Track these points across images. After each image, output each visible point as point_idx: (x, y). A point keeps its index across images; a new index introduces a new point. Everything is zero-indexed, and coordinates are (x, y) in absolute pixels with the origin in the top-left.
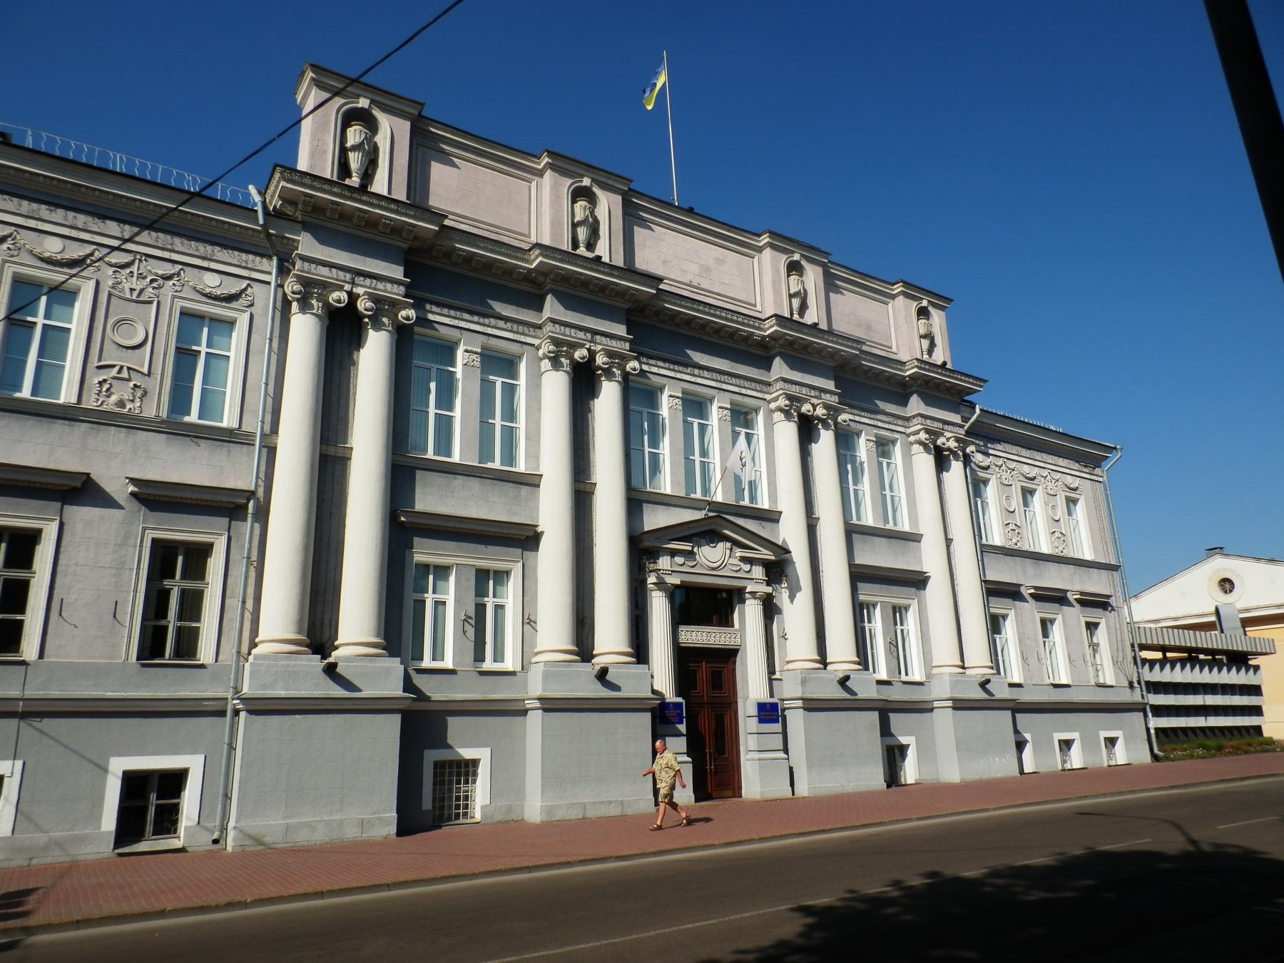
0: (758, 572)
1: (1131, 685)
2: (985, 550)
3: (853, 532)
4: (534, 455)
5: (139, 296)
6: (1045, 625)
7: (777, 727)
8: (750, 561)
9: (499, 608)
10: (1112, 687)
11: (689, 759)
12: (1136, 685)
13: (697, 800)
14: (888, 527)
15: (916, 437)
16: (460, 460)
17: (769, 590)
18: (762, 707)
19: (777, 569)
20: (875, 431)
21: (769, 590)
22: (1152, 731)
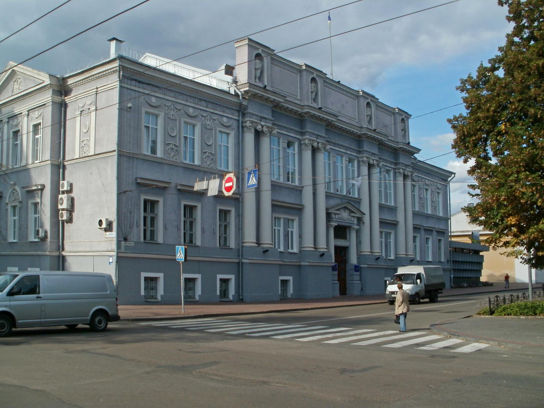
0: (356, 222)
1: (448, 261)
2: (415, 214)
3: (381, 207)
4: (300, 180)
5: (210, 127)
6: (427, 239)
7: (358, 273)
8: (354, 217)
9: (292, 232)
10: (443, 262)
11: (338, 282)
12: (449, 262)
13: (340, 295)
14: (388, 204)
15: (399, 171)
16: (283, 182)
17: (358, 227)
18: (356, 267)
19: (360, 220)
20: (386, 168)
21: (358, 227)
22: (452, 278)
